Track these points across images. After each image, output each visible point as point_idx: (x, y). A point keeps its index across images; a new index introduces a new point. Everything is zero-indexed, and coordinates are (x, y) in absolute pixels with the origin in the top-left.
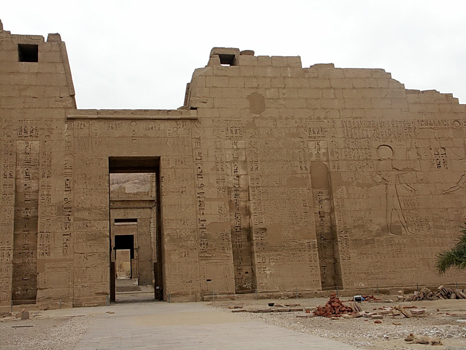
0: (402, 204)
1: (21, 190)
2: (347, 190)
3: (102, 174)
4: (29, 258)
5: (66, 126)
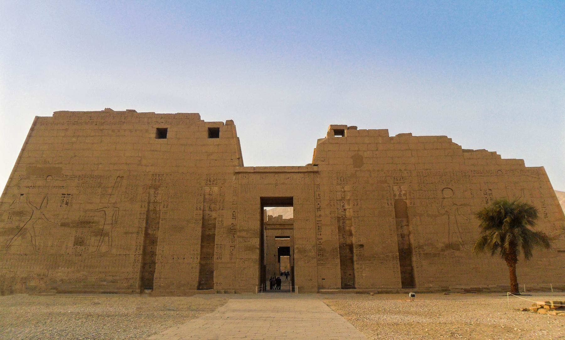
0: (460, 229)
1: (207, 217)
2: (420, 220)
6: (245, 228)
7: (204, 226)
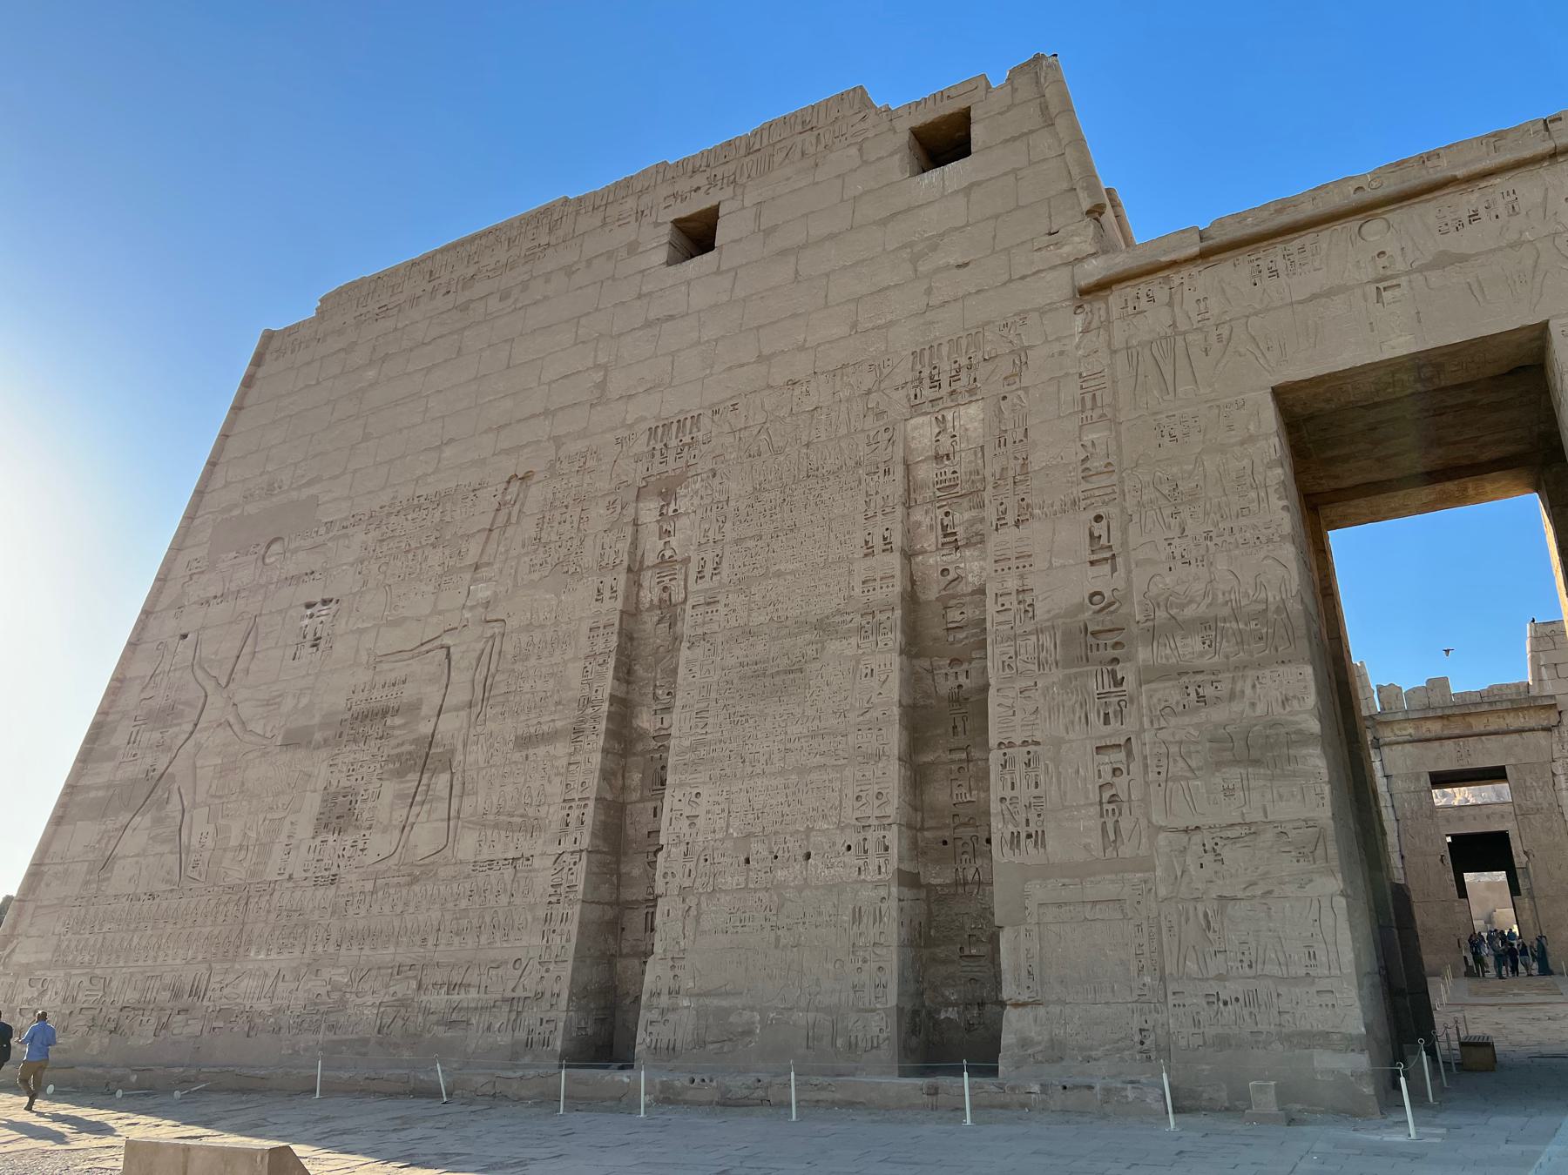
1: (932, 593)
3: (1246, 462)
4: (979, 862)
5: (1079, 322)
6: (1190, 612)
7: (914, 645)
